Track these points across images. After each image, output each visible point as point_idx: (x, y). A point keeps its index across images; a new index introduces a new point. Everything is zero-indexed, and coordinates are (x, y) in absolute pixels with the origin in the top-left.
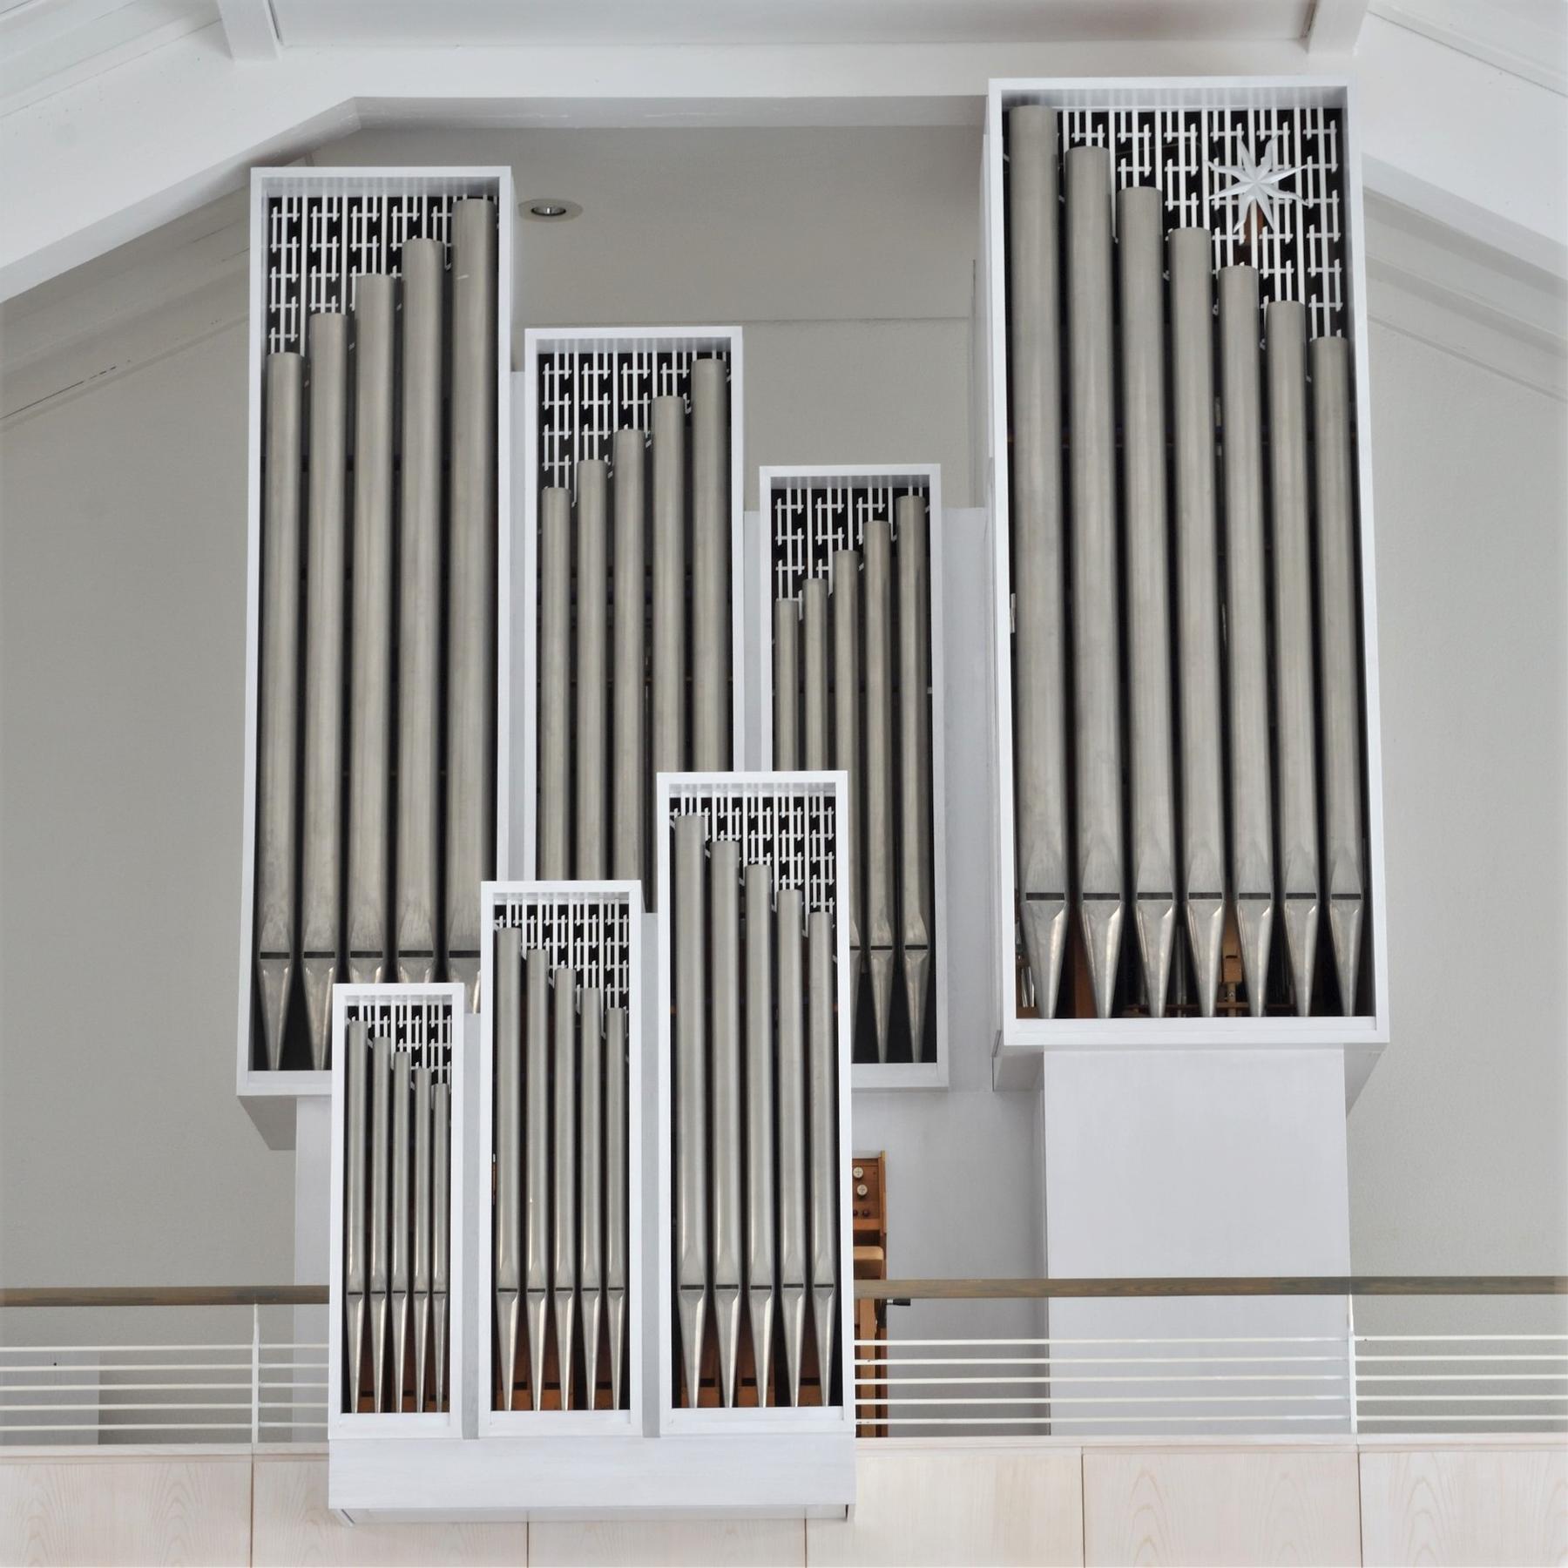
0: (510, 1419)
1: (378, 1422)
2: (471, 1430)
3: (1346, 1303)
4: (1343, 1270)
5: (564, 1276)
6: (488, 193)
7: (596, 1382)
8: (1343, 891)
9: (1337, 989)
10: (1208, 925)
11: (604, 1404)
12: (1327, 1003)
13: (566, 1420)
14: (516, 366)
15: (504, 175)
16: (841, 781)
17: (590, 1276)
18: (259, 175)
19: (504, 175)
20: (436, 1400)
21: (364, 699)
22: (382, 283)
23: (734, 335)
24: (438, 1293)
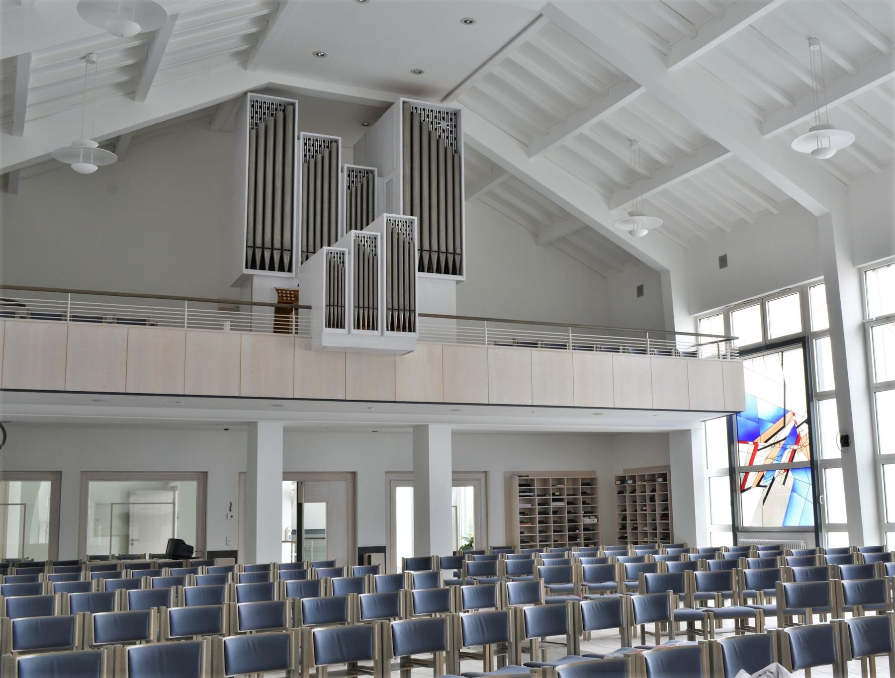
0: (357, 331)
1: (332, 330)
2: (349, 333)
3: (455, 320)
4: (455, 314)
5: (366, 305)
6: (293, 104)
7: (372, 325)
8: (457, 254)
9: (456, 270)
10: (435, 257)
11: (373, 329)
12: (454, 273)
13: (366, 332)
14: (299, 138)
15: (297, 102)
16: (416, 219)
17: (371, 306)
18: (249, 94)
19: (297, 102)
20: (342, 327)
21: (269, 196)
22: (272, 119)
23: (340, 138)
24: (375, 308)
